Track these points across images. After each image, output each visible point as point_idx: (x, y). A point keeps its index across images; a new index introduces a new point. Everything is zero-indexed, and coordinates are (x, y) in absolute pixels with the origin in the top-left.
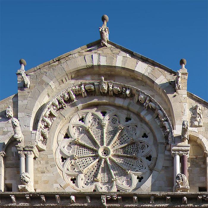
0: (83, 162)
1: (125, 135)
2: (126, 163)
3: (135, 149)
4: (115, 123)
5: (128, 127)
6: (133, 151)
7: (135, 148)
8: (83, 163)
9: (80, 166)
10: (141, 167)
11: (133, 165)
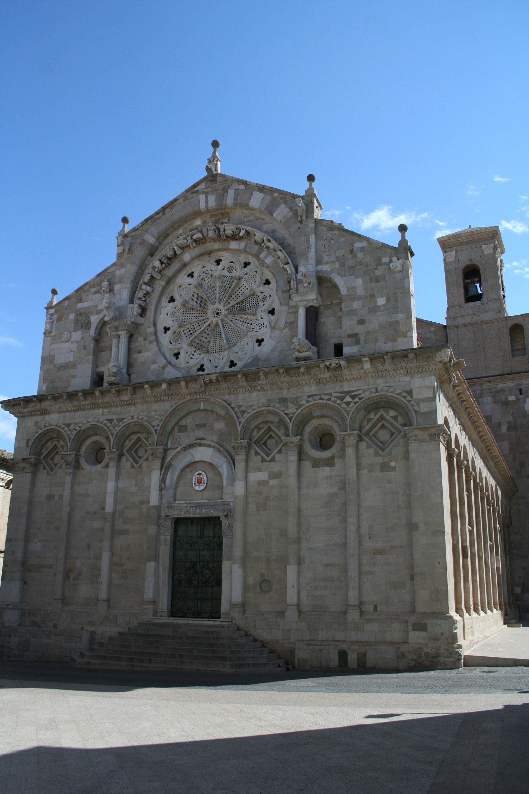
0: (190, 329)
1: (243, 285)
2: (243, 322)
3: (254, 302)
4: (231, 272)
5: (246, 274)
6: (253, 305)
7: (254, 300)
8: (190, 331)
9: (186, 335)
10: (261, 325)
11: (251, 324)
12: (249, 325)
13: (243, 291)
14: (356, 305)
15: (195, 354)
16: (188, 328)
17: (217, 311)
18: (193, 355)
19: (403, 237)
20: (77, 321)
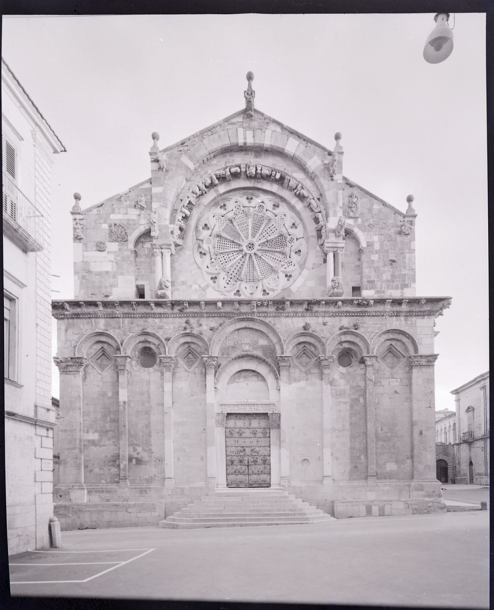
8: (225, 259)
9: (222, 262)
12: (278, 262)
13: (273, 231)
14: (375, 257)
15: (231, 280)
16: (224, 257)
17: (250, 245)
18: (229, 281)
19: (410, 206)
20: (111, 232)
